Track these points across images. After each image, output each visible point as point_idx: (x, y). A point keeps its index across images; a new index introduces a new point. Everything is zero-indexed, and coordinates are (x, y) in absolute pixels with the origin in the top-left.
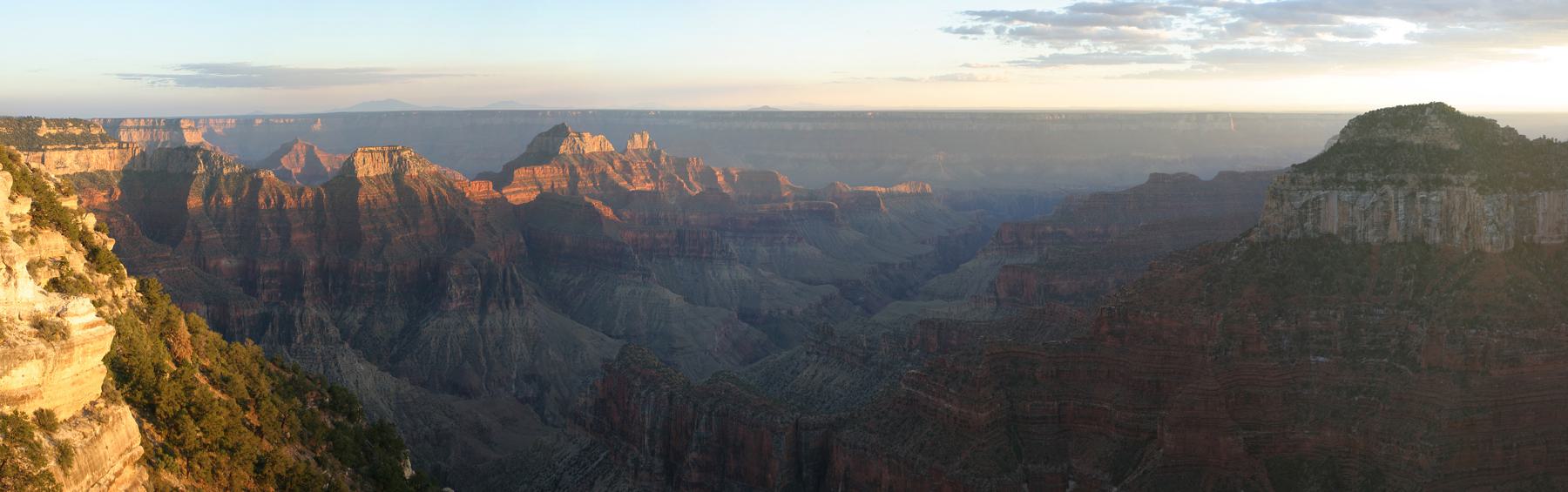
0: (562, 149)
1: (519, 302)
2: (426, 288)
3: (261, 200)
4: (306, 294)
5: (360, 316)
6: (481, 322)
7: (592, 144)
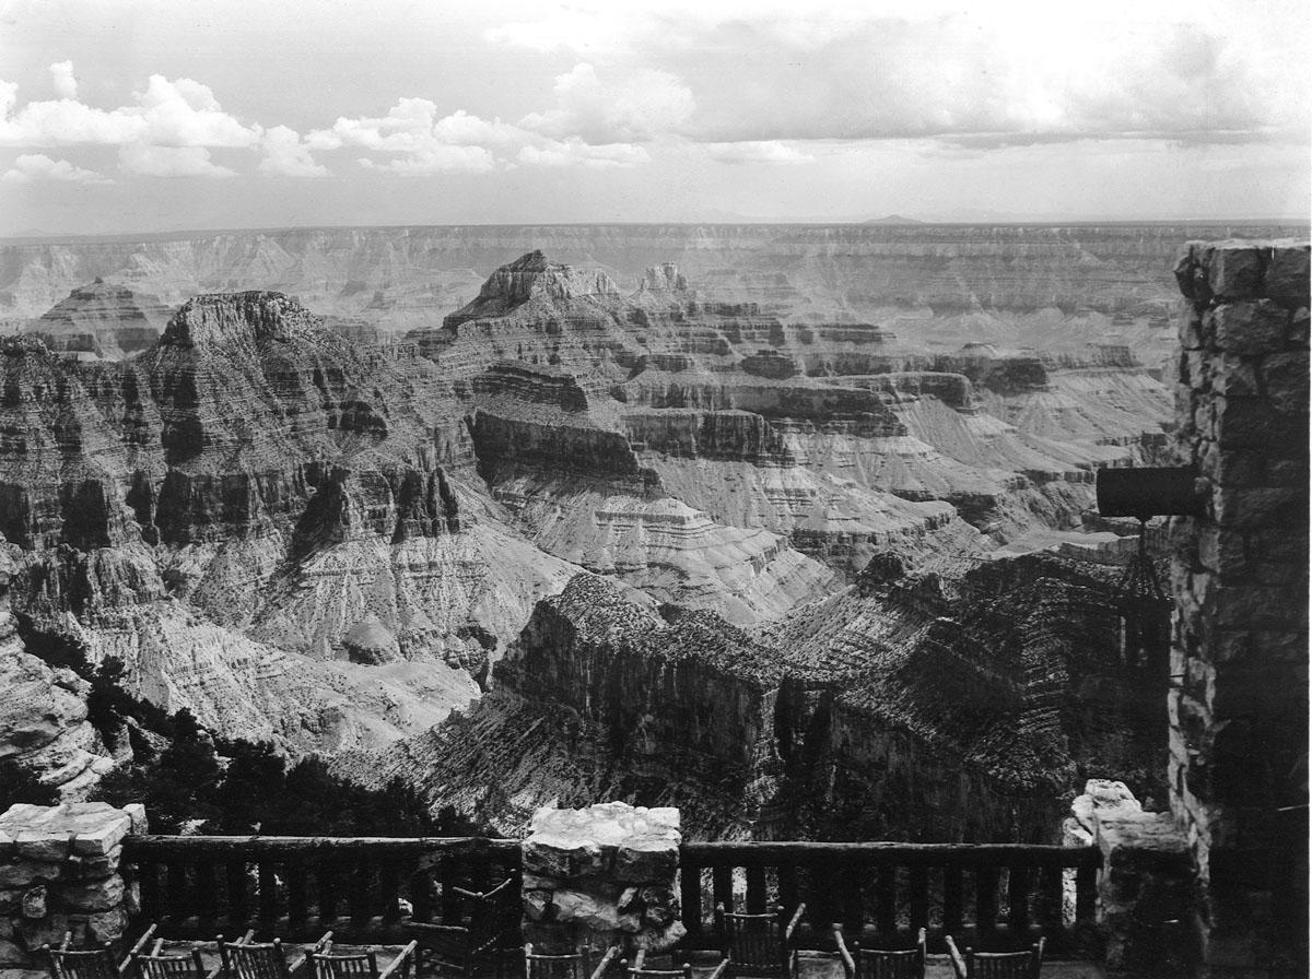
6: (394, 555)
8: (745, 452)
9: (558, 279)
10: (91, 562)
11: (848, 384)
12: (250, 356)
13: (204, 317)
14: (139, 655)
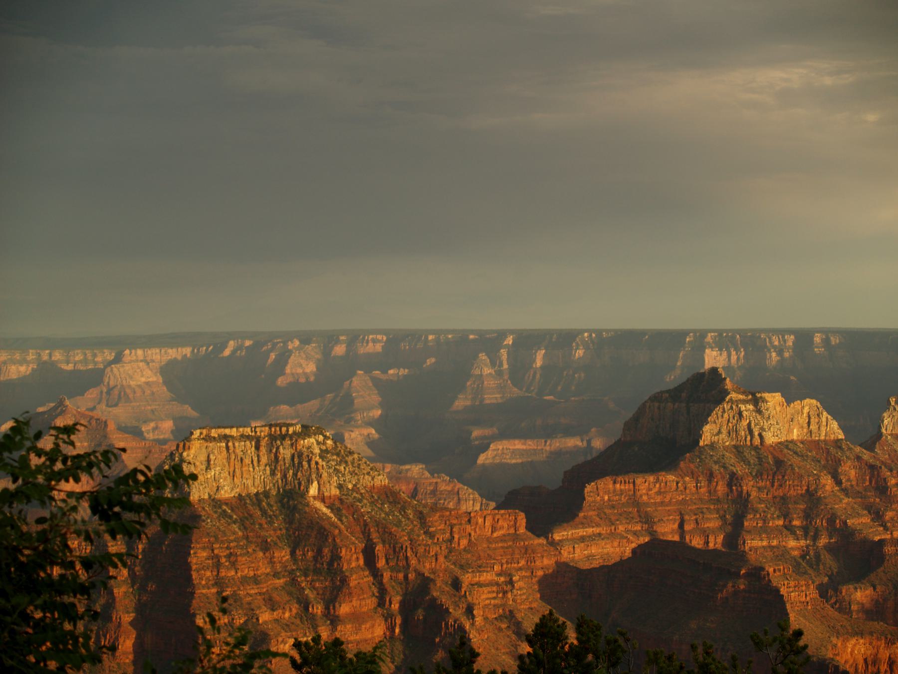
0: (708, 433)
7: (786, 421)
9: (745, 414)
12: (271, 523)
13: (209, 461)
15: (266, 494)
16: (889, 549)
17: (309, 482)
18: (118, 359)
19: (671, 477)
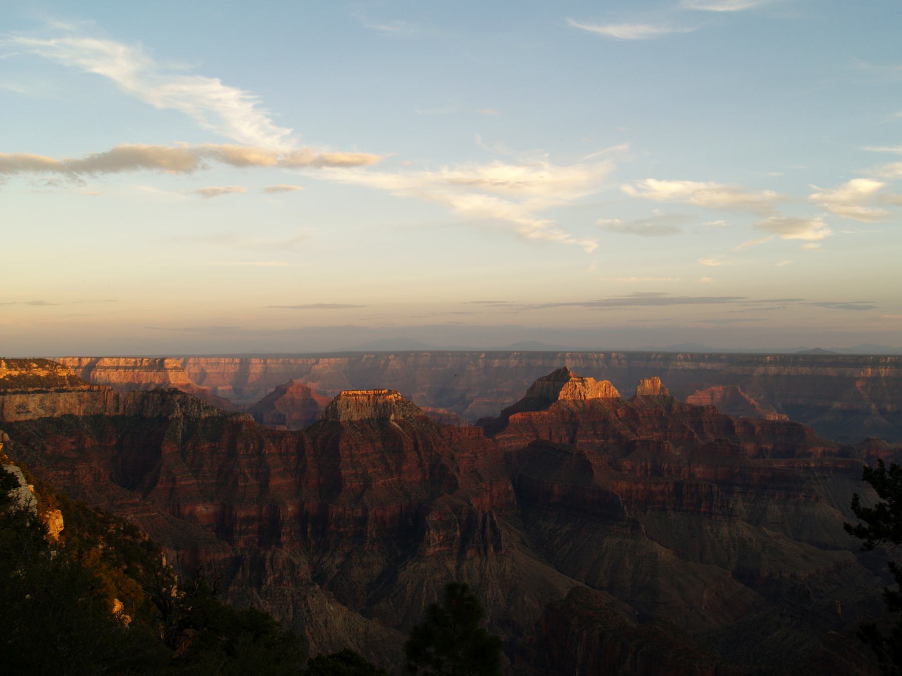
0: (562, 395)
1: (497, 548)
2: (407, 533)
3: (240, 445)
4: (284, 539)
5: (338, 561)
6: (458, 568)
7: (595, 390)
8: (703, 510)
10: (268, 557)
11: (780, 464)
14: (293, 619)
15: (373, 419)
16: (637, 444)
17: (391, 414)
18: (317, 363)
19: (546, 413)
